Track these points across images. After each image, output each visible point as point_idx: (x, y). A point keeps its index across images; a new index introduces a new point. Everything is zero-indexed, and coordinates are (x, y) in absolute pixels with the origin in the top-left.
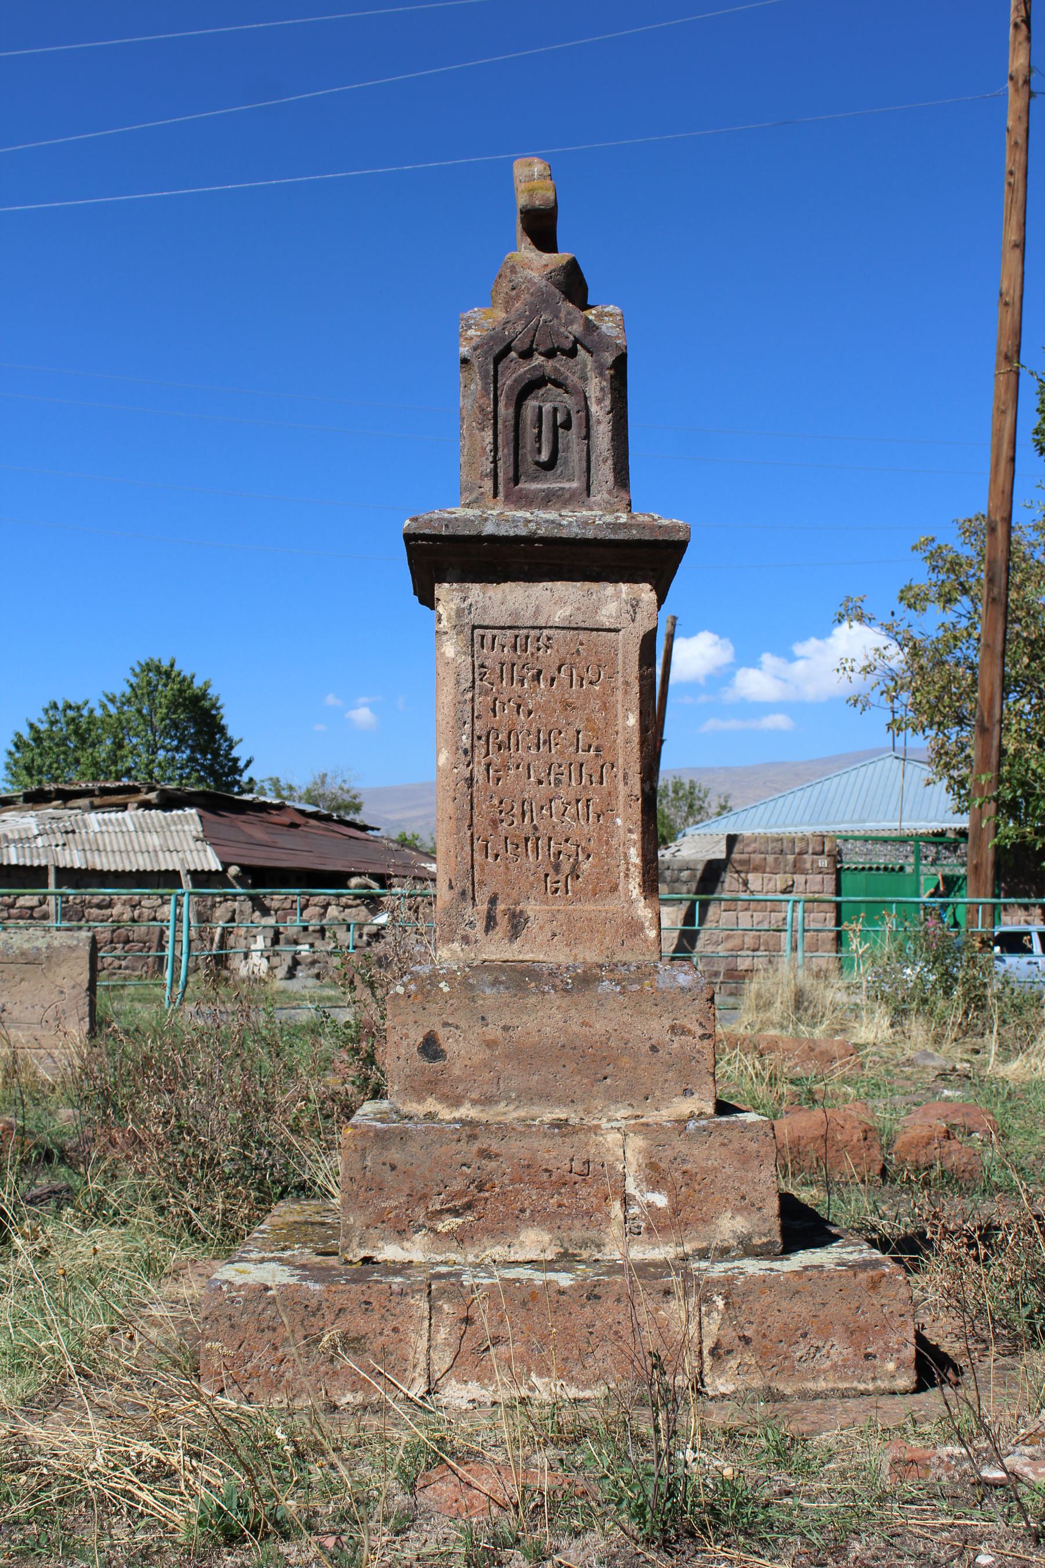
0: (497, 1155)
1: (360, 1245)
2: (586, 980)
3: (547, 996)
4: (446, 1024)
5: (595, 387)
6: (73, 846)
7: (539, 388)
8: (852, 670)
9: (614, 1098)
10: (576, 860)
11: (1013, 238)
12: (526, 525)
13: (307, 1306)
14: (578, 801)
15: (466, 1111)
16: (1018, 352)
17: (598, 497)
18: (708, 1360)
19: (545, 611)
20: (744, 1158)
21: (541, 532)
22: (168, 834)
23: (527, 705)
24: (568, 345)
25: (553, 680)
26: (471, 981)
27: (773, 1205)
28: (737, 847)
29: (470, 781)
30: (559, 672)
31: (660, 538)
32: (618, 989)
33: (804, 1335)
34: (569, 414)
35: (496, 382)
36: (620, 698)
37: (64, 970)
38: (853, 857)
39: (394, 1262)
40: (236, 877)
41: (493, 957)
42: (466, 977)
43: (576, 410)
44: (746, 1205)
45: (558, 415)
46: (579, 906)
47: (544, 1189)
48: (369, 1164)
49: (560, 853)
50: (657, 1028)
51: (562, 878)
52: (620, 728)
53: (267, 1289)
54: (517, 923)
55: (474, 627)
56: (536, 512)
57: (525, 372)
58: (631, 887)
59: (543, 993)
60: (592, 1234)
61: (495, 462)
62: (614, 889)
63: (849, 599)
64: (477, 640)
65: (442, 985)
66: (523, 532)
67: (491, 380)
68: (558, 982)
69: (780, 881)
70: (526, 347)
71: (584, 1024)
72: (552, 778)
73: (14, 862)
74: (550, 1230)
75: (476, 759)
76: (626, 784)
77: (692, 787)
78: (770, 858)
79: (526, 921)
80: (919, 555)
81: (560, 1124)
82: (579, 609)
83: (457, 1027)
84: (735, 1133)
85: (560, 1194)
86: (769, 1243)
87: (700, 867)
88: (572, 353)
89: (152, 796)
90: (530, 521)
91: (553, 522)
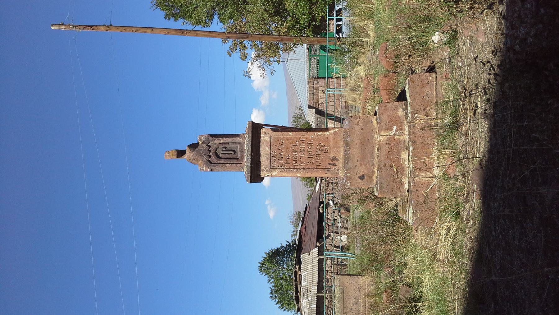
0: (385, 163)
1: (405, 193)
2: (347, 144)
3: (351, 152)
4: (357, 174)
5: (217, 141)
6: (311, 289)
7: (217, 154)
8: (264, 74)
9: (373, 137)
10: (321, 146)
11: (150, 31)
12: (248, 157)
13: (417, 204)
14: (308, 146)
15: (376, 170)
16: (181, 30)
17: (242, 141)
18: (429, 118)
19: (266, 152)
20: (386, 110)
22: (308, 263)
23: (287, 157)
24: (208, 147)
25: (282, 151)
26: (347, 169)
27: (396, 103)
28: (312, 105)
29: (304, 169)
30: (280, 149)
31: (251, 127)
32: (349, 137)
33: (424, 97)
34: (223, 147)
35: (216, 163)
36: (286, 136)
37: (346, 283)
38: (315, 75)
39: (408, 186)
40: (320, 244)
41: (342, 164)
42: (346, 170)
44: (396, 109)
45: (223, 149)
46: (331, 145)
47: (392, 153)
48: (387, 191)
49: (319, 150)
50: (357, 128)
52: (292, 136)
53: (413, 212)
54: (335, 159)
55: (270, 168)
57: (214, 157)
58: (327, 134)
59: (350, 153)
60: (402, 142)
61: (234, 164)
62: (327, 138)
63: (244, 75)
64: (273, 167)
65: (348, 175)
66: (250, 157)
67: (216, 164)
68: (347, 150)
69: (321, 94)
71: (356, 144)
72: (303, 151)
73: (315, 306)
74: (401, 152)
75: (299, 168)
76: (304, 135)
77: (294, 117)
78: (315, 97)
79: (334, 157)
80: (232, 56)
81: (378, 150)
82: (266, 145)
83: (357, 172)
84: (380, 111)
85: (393, 150)
86: (404, 104)
87: (317, 116)
88: (210, 146)
89: (297, 267)
91: (248, 151)
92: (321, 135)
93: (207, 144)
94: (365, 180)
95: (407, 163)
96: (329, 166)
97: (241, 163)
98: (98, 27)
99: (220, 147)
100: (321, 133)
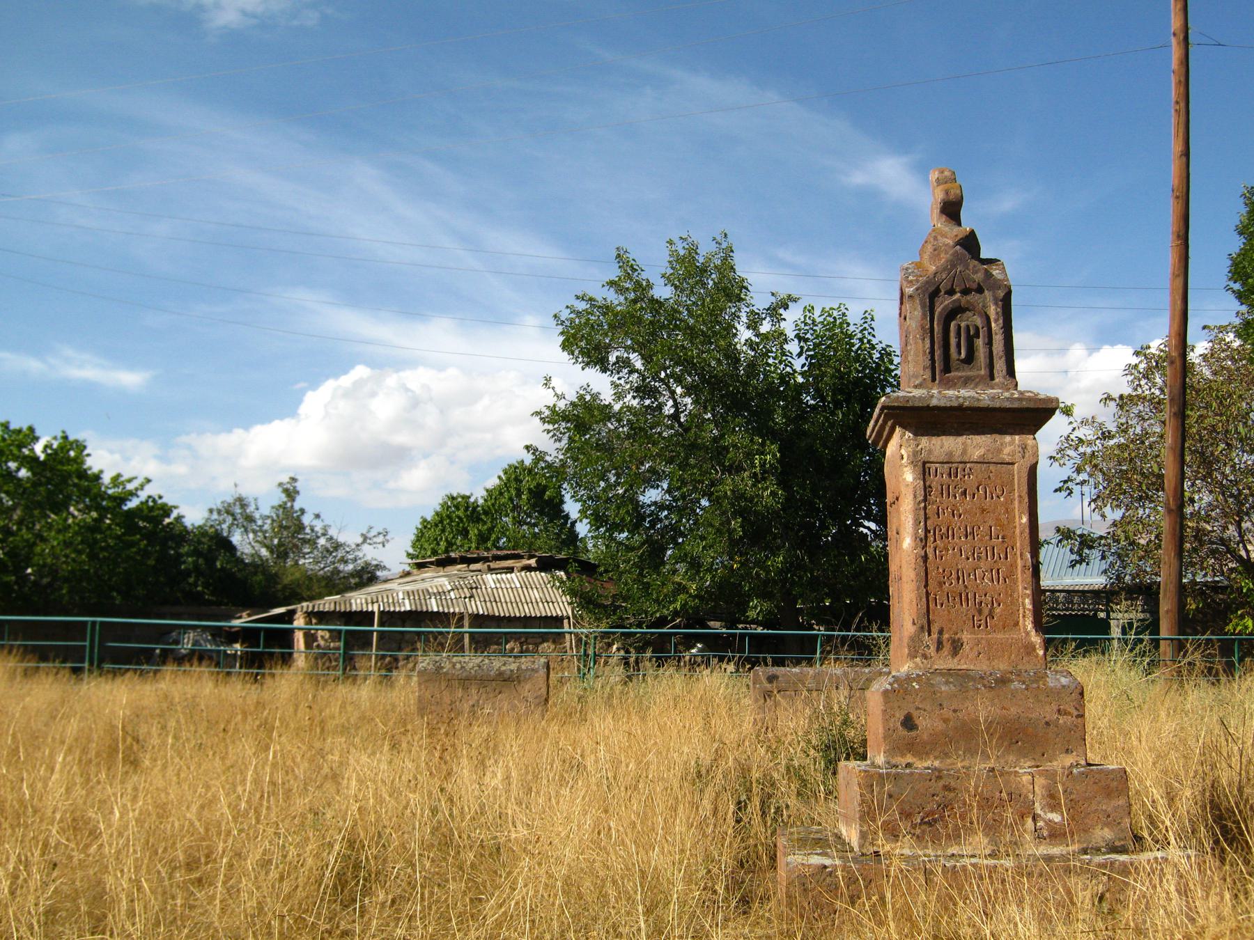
0: (954, 789)
2: (1003, 681)
4: (917, 708)
5: (993, 311)
6: (477, 599)
9: (1023, 754)
19: (970, 450)
21: (967, 404)
22: (545, 589)
23: (958, 510)
24: (975, 286)
25: (974, 495)
29: (925, 558)
42: (928, 679)
46: (994, 635)
50: (1049, 712)
51: (983, 618)
54: (956, 647)
55: (924, 463)
59: (978, 689)
62: (1017, 624)
66: (955, 404)
68: (986, 682)
70: (949, 287)
71: (1003, 708)
73: (435, 609)
79: (962, 645)
82: (988, 450)
89: (533, 562)
92: (1024, 608)
94: (902, 732)
95: (955, 852)
96: (935, 629)
99: (979, 321)
100: (1030, 607)
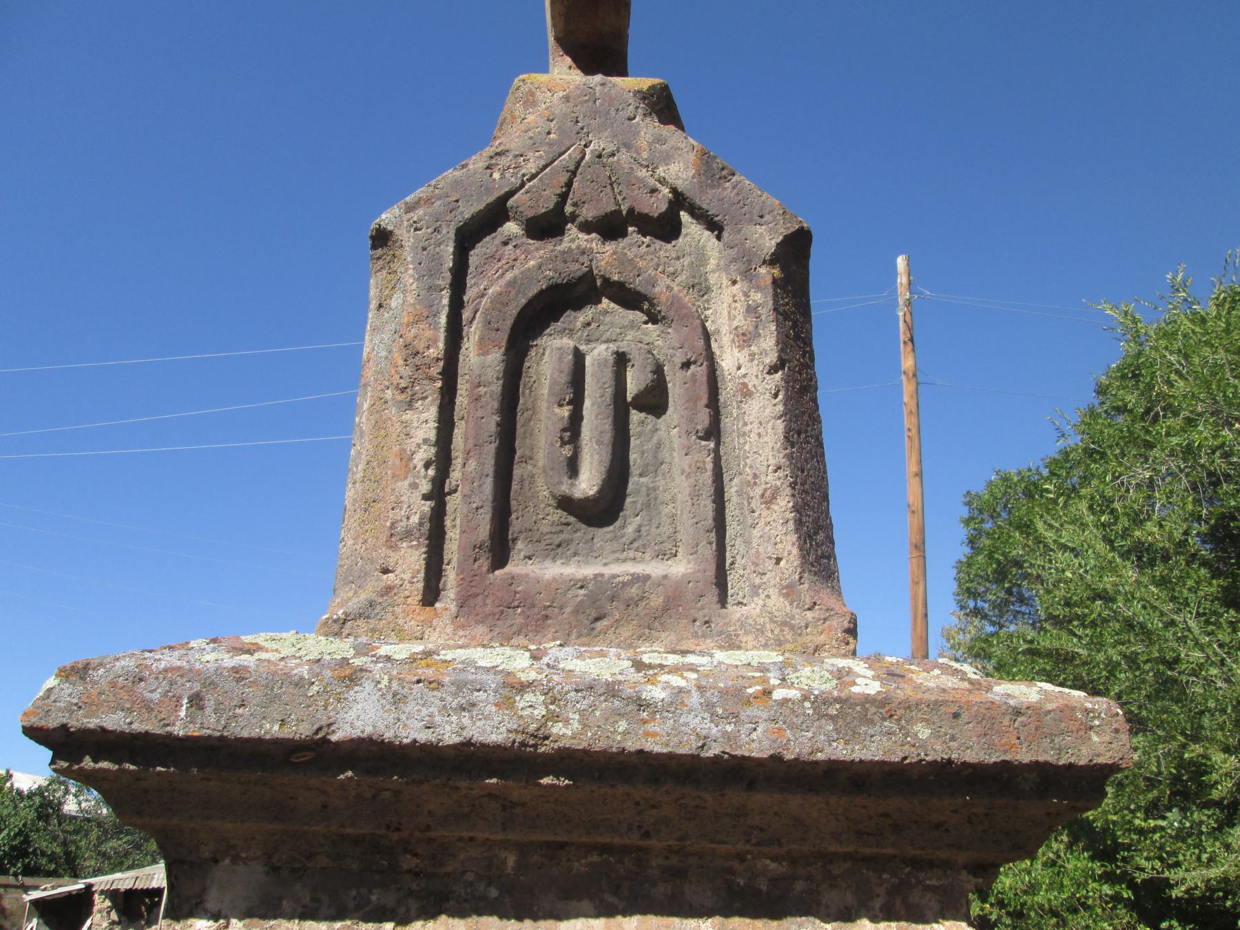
7: (578, 306)
11: (914, 470)
12: (506, 703)
17: (754, 608)
24: (657, 205)
31: (1024, 756)
34: (659, 371)
43: (679, 359)
56: (554, 650)
61: (438, 494)
67: (445, 279)
70: (547, 203)
90: (523, 687)
91: (612, 690)
93: (706, 201)
97: (431, 594)
98: (912, 354)
